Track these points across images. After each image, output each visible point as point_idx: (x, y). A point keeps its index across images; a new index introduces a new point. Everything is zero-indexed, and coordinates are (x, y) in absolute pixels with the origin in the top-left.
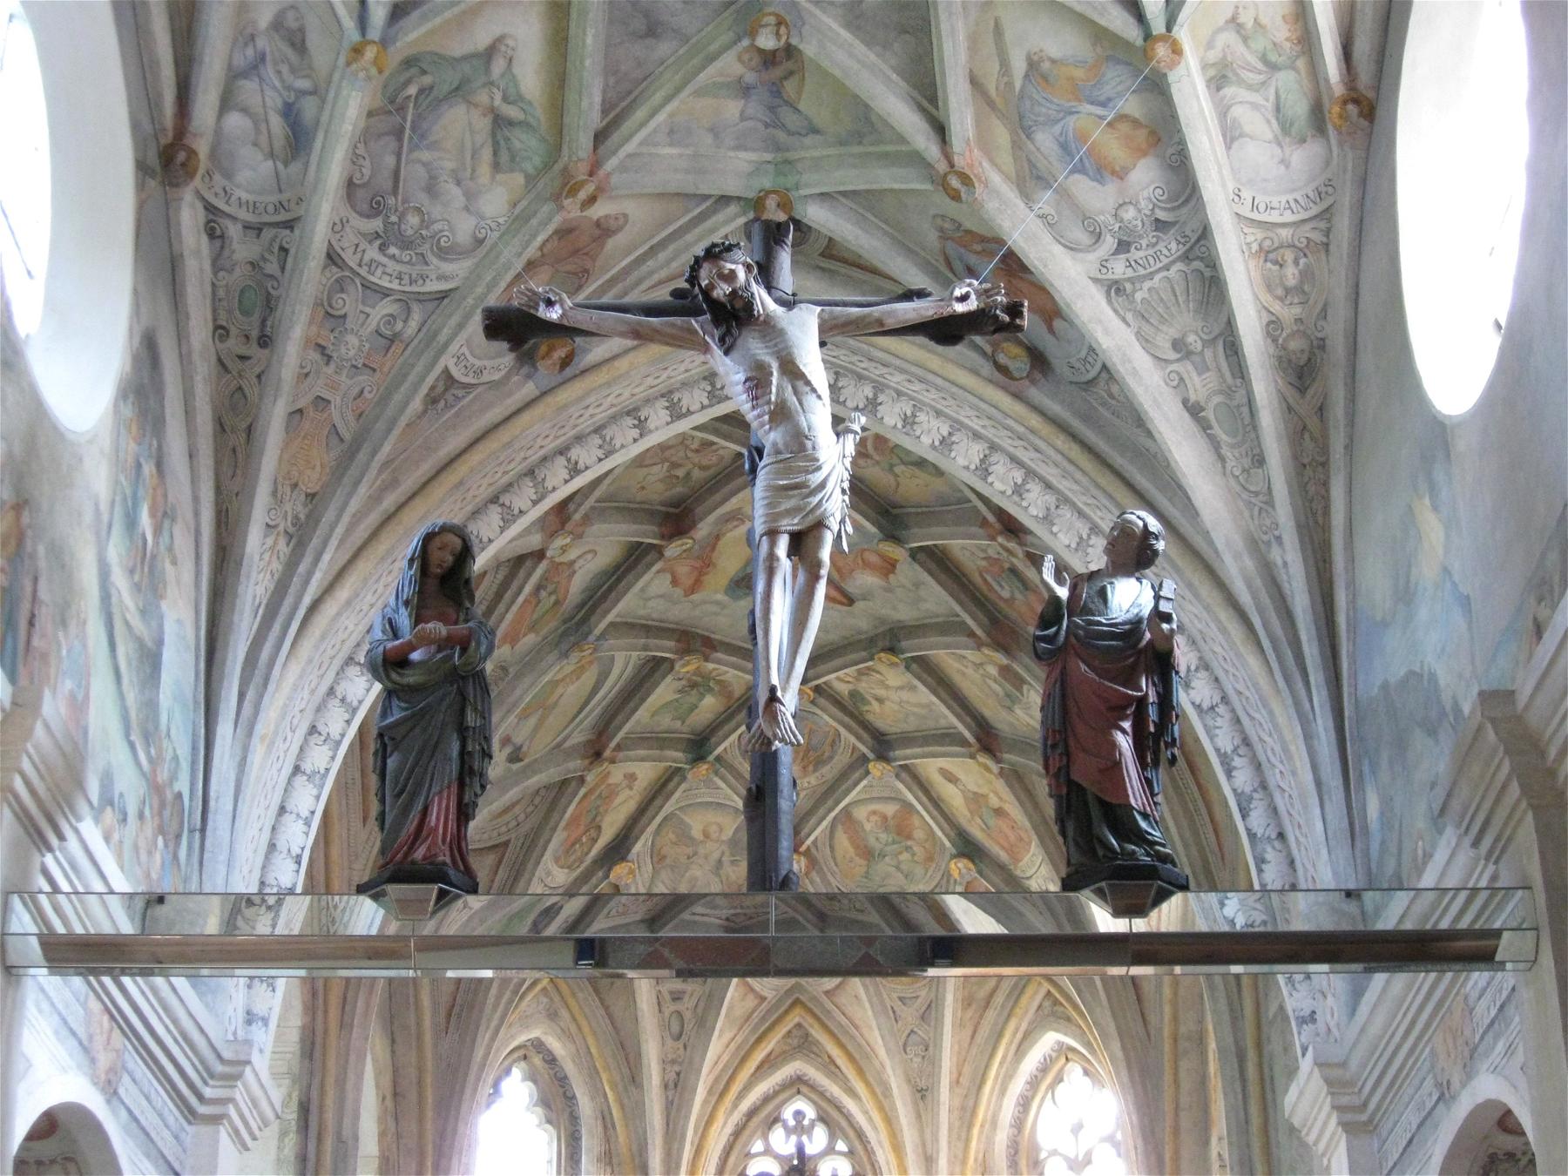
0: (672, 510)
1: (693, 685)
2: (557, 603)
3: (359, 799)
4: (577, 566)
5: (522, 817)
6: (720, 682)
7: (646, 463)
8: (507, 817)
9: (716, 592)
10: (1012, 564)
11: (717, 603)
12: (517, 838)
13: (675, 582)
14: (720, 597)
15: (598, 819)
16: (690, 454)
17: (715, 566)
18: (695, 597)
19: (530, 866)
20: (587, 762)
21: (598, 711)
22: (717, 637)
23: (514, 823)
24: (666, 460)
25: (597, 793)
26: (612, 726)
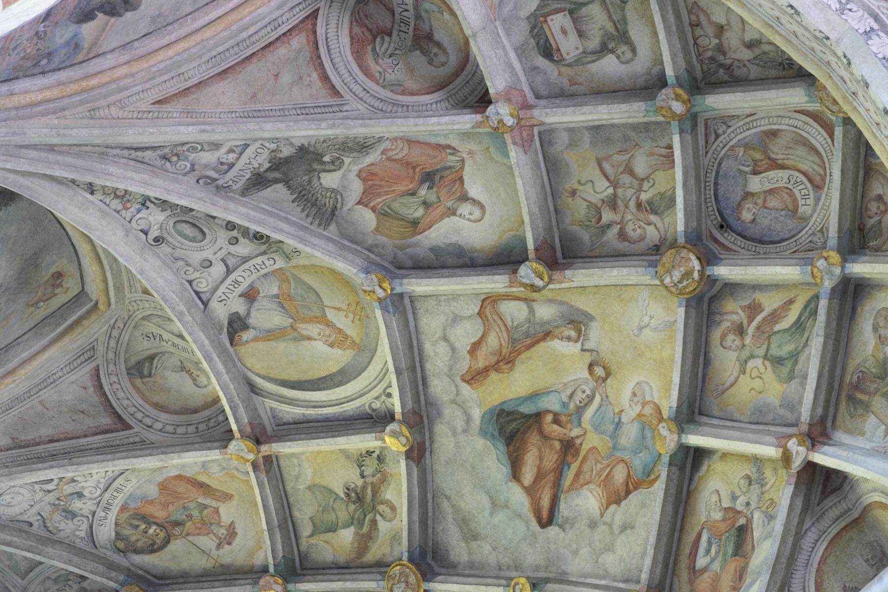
0: (559, 253)
1: (360, 499)
2: (415, 223)
3: (173, 91)
4: (465, 209)
5: (158, 426)
6: (374, 522)
7: (607, 166)
8: (153, 412)
9: (479, 406)
10: (750, 521)
11: (468, 419)
12: (137, 434)
13: (475, 348)
14: (476, 414)
15: (177, 531)
16: (632, 204)
17: (511, 369)
18: (465, 388)
19: (118, 455)
20: (248, 430)
21: (297, 412)
22: (428, 461)
23: (148, 421)
24: (615, 184)
25: (207, 501)
26: (290, 437)
